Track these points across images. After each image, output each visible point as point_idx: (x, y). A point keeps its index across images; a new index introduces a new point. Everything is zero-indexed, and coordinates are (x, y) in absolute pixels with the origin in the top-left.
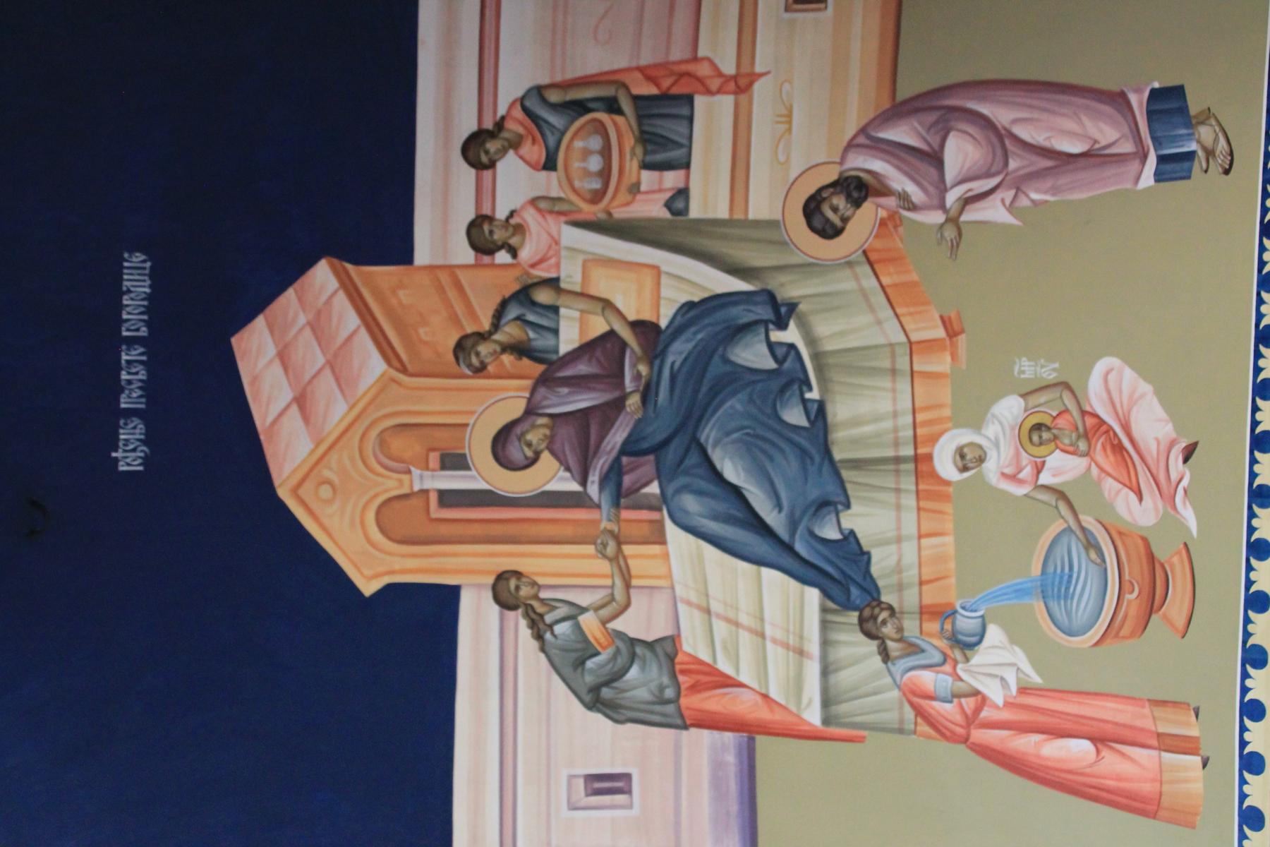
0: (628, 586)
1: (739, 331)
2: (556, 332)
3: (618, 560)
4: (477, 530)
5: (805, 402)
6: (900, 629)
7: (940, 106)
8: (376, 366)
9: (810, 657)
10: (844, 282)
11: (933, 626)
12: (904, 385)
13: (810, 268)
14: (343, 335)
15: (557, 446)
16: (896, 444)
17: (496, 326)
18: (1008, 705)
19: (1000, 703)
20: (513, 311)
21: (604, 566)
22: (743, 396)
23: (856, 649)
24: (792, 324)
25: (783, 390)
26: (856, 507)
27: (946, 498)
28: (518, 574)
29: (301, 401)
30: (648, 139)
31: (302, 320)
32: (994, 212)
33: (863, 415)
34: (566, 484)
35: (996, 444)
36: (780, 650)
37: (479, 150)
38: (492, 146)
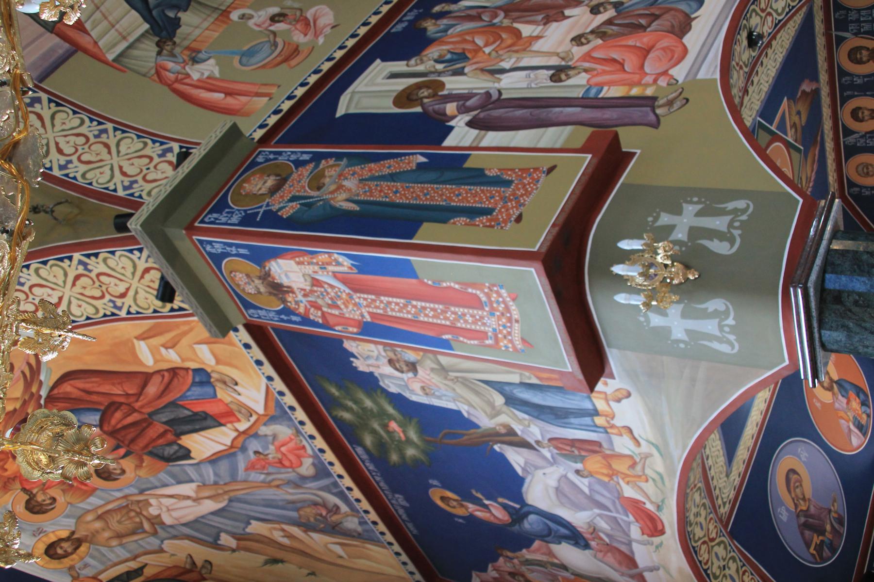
6: (173, 49)
9: (127, 40)
11: (188, 53)
23: (149, 49)
26: (188, 13)
35: (260, 17)
36: (116, 34)
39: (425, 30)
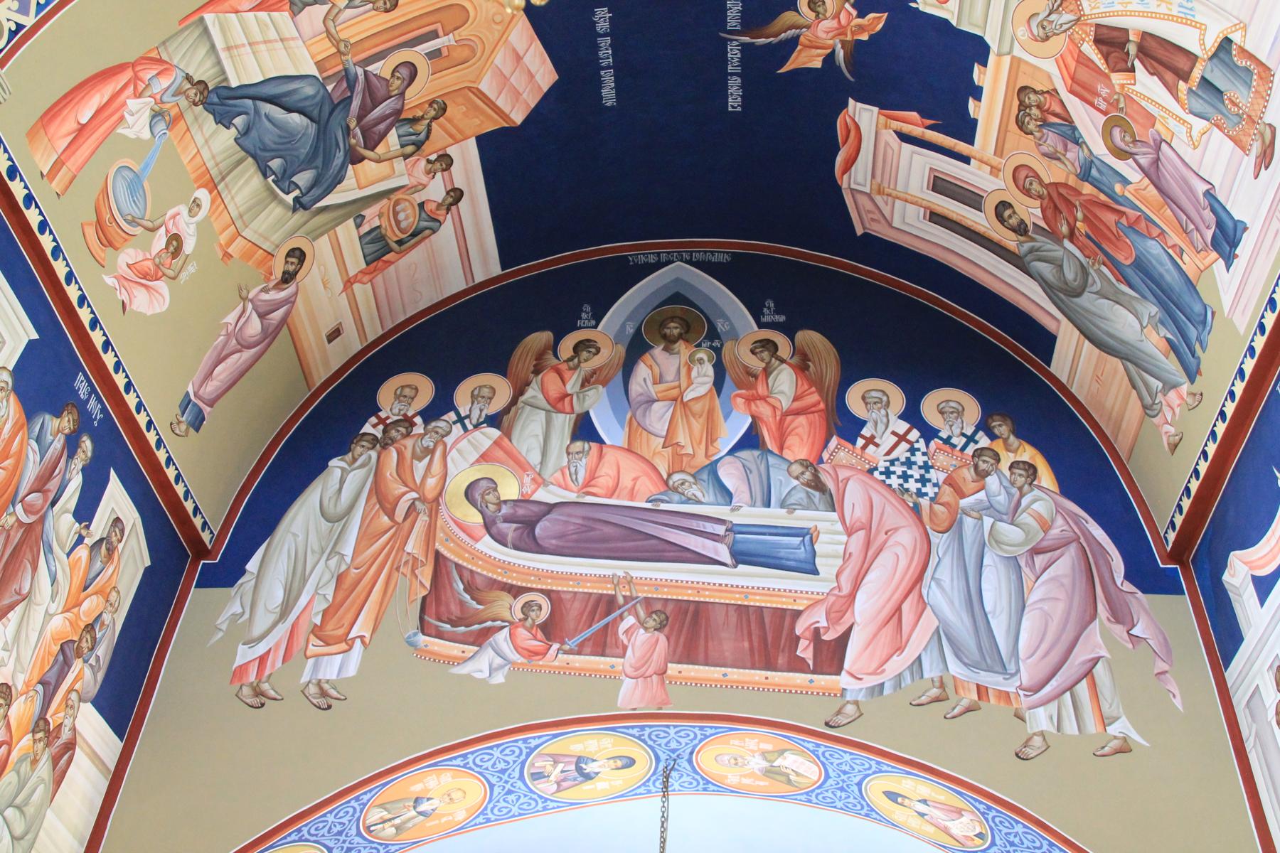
0: (328, 31)
1: (315, 184)
2: (399, 136)
3: (335, 41)
4: (414, 25)
5: (274, 173)
6: (187, 97)
7: (269, 335)
8: (485, 86)
9: (224, 50)
10: (276, 237)
11: (174, 112)
12: (234, 214)
13: (292, 234)
14: (502, 95)
15: (384, 83)
16: (227, 186)
17: (429, 126)
18: (125, 104)
19: (129, 102)
20: (422, 136)
21: (343, 36)
22: (302, 157)
23: (203, 70)
24: (291, 203)
25: (285, 171)
26: (232, 141)
27: (196, 181)
28: (387, 11)
29: (518, 58)
30: (382, 238)
31: (525, 95)
32: (231, 318)
33: (247, 185)
34: (373, 68)
35: (187, 224)
36: (239, 42)
37: (456, 195)
38: (450, 200)
39: (58, 414)
